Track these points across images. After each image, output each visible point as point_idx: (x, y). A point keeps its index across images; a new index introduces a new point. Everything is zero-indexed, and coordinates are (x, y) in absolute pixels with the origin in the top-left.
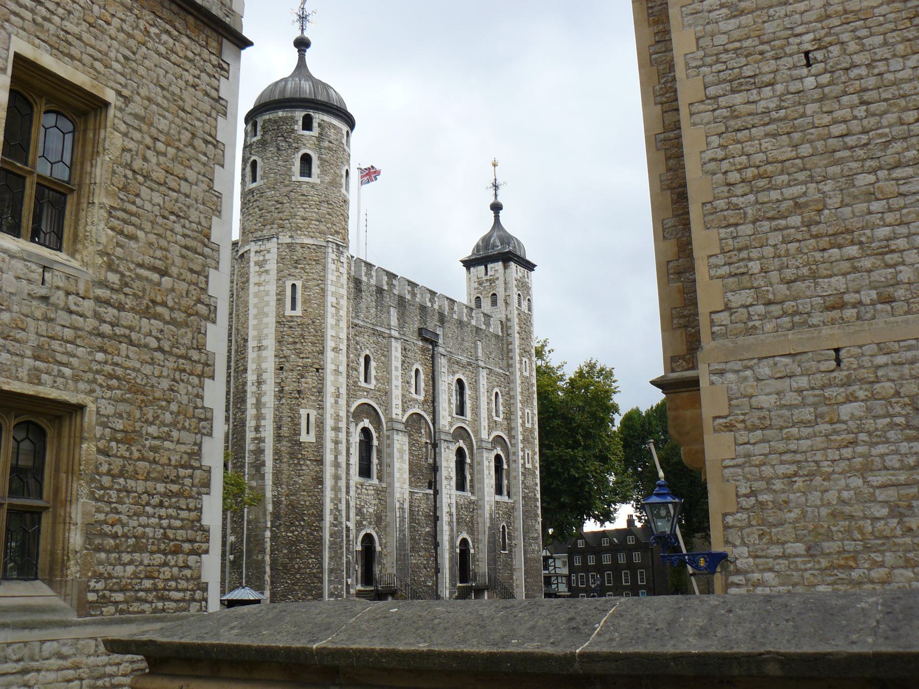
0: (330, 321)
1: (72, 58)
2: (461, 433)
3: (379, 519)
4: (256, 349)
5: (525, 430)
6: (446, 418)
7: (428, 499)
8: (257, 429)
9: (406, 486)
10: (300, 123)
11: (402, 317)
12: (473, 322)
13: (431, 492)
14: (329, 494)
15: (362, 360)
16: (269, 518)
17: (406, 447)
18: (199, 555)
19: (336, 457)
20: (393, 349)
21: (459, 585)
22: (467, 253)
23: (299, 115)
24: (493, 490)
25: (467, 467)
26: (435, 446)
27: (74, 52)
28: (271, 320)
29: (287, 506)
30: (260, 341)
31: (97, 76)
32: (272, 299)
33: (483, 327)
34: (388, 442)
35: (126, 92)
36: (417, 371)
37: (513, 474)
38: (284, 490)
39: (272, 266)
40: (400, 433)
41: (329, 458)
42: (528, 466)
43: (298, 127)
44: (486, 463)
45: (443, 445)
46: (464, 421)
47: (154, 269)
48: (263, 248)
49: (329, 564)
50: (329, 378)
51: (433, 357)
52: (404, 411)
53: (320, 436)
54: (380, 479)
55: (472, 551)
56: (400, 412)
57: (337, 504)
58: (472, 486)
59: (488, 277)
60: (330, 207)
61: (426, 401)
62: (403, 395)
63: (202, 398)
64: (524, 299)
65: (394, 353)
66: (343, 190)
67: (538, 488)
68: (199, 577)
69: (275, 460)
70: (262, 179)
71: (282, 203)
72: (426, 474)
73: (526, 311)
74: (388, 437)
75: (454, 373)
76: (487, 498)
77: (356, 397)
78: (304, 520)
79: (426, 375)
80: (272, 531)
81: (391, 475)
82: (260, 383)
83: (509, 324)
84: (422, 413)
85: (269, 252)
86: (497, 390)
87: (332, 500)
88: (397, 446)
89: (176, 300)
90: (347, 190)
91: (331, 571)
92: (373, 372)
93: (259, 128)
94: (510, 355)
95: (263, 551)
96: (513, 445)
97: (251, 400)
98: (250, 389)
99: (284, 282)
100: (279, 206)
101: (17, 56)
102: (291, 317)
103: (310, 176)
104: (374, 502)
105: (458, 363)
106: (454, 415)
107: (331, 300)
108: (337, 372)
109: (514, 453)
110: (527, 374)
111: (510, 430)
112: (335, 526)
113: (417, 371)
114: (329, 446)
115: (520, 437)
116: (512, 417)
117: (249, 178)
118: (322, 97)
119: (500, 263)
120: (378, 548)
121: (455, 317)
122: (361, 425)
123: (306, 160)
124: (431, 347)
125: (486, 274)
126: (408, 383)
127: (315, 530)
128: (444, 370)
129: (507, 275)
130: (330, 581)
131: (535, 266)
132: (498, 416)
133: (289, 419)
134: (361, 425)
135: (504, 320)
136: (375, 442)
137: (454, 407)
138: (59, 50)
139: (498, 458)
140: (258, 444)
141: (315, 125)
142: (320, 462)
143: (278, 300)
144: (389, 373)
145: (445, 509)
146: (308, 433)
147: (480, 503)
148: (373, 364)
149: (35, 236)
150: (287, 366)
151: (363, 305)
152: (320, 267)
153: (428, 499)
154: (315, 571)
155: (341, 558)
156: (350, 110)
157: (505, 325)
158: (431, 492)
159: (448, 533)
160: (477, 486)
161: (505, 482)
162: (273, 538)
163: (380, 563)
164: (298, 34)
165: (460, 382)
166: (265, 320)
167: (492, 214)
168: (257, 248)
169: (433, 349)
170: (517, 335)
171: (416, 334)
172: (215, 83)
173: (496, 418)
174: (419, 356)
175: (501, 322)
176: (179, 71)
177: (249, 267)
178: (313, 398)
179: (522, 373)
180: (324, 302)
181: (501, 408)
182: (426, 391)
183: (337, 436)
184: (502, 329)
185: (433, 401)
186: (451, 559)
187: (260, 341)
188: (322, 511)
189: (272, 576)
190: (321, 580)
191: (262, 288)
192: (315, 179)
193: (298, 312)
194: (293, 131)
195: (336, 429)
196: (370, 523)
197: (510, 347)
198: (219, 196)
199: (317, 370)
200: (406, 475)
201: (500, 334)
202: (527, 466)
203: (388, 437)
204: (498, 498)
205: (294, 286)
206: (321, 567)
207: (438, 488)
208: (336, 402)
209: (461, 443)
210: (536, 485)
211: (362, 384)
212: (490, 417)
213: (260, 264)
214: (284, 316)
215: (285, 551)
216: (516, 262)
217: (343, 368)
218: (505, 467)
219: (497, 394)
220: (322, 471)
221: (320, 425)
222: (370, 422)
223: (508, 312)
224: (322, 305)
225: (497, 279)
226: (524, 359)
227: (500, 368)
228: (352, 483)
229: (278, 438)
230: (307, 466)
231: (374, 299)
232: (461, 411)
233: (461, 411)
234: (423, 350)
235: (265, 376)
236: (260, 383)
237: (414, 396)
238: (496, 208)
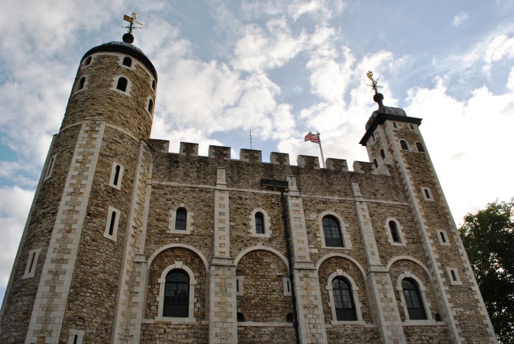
83: (398, 165)
124: (279, 193)
131: (421, 120)
144: (212, 218)
146: (30, 271)
158: (291, 324)
182: (274, 230)
201: (389, 174)
202: (453, 283)
216: (391, 119)
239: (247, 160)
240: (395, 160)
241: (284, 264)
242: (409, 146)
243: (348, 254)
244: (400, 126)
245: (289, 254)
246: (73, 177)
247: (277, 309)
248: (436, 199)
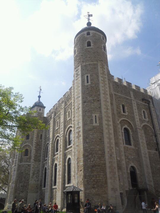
9: (146, 149)
13: (158, 152)
14: (106, 145)
19: (109, 131)
26: (156, 136)
41: (105, 131)
50: (103, 103)
53: (101, 123)
54: (135, 146)
56: (139, 123)
57: (111, 150)
65: (133, 105)
77: (120, 117)
88: (139, 134)
99: (84, 76)
108: (106, 101)
113: (144, 112)
114: (105, 127)
122: (124, 127)
124: (147, 105)
126: (141, 115)
136: (131, 133)
144: (133, 111)
146: (96, 122)
148: (126, 108)
164: (88, 22)
182: (149, 118)
193: (89, 83)
195: (108, 121)
205: (87, 76)
214: (85, 86)
215: (90, 170)
221: (101, 119)
222: (128, 126)
237: (144, 119)
239: (137, 90)
241: (152, 131)
246: (102, 87)
247: (153, 146)
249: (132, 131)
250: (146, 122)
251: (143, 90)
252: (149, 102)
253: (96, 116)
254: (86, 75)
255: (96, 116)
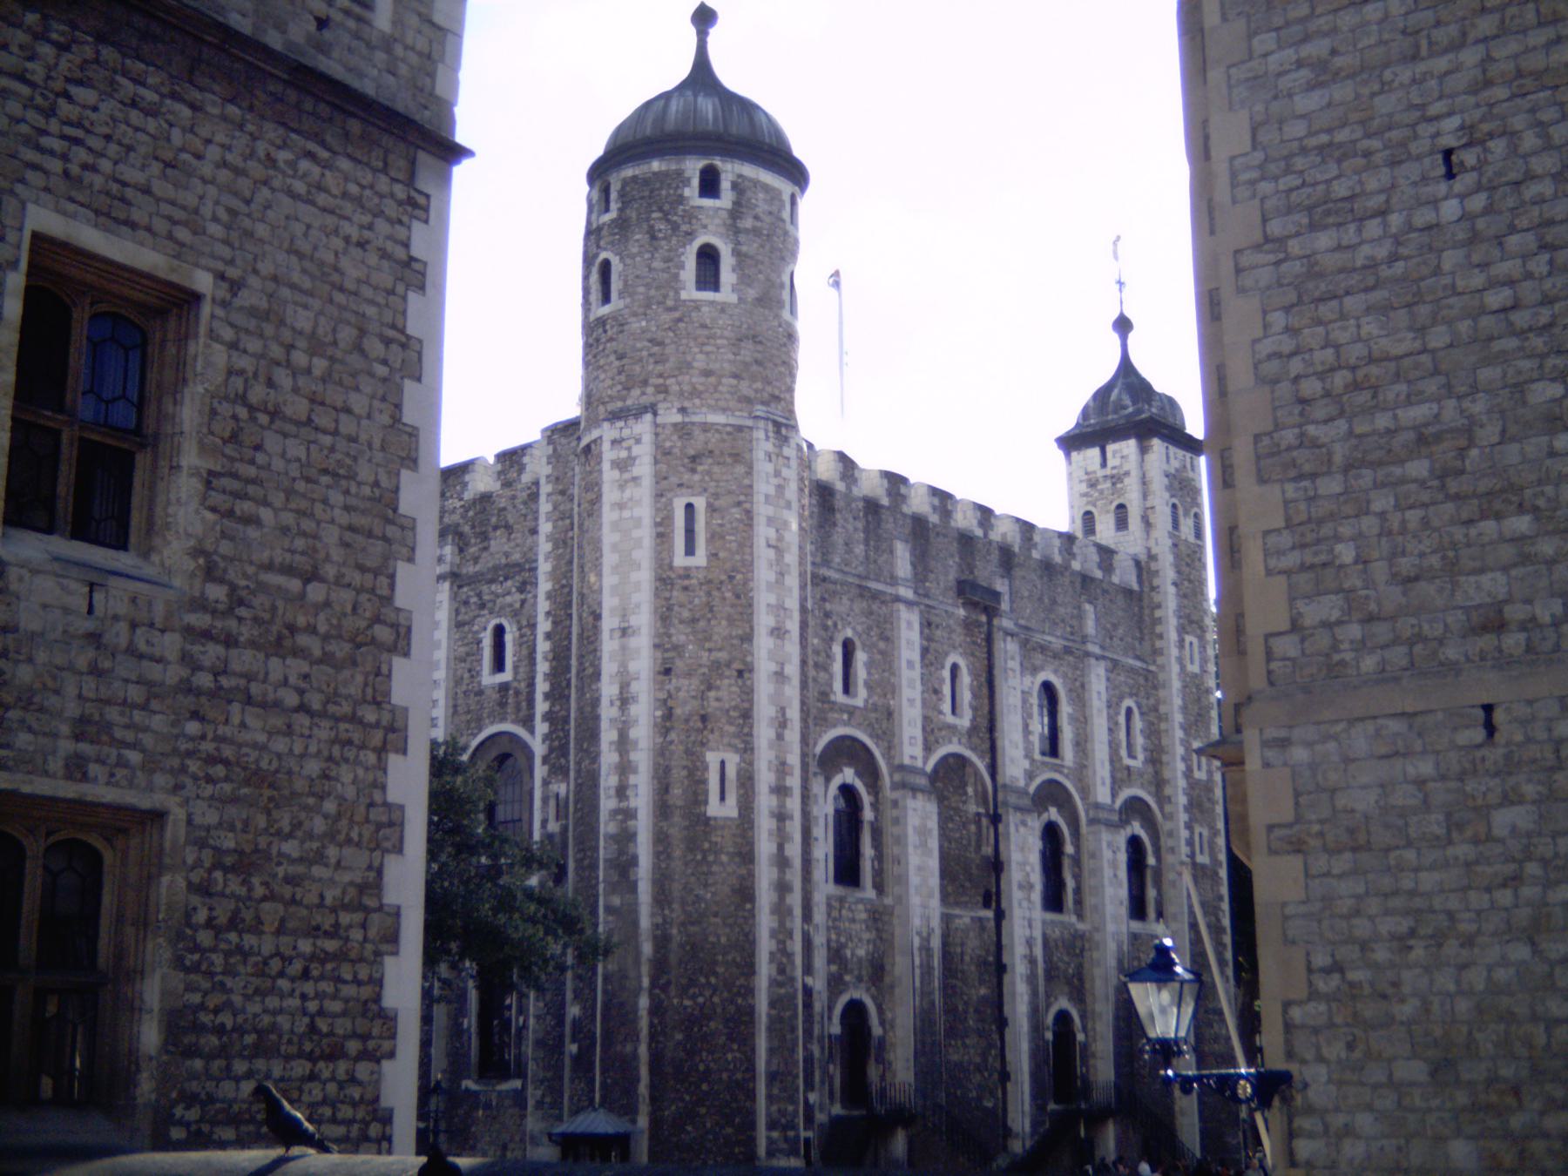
0: (764, 574)
1: (133, 225)
2: (1051, 794)
3: (877, 971)
4: (617, 634)
5: (1193, 784)
6: (1018, 760)
7: (983, 928)
8: (621, 791)
9: (935, 903)
10: (696, 182)
11: (921, 558)
12: (1076, 565)
13: (989, 914)
15: (837, 650)
16: (645, 969)
17: (933, 824)
18: (378, 1062)
19: (781, 847)
20: (903, 625)
21: (1052, 1106)
22: (1067, 421)
23: (693, 167)
24: (1124, 911)
25: (1066, 862)
26: (996, 819)
27: (137, 215)
28: (644, 576)
29: (682, 946)
30: (624, 617)
31: (180, 251)
32: (646, 534)
33: (1099, 574)
34: (895, 813)
35: (233, 273)
36: (955, 669)
37: (1170, 876)
38: (676, 913)
39: (644, 468)
40: (920, 796)
41: (765, 847)
42: (1203, 859)
43: (692, 191)
44: (1107, 854)
45: (1012, 819)
46: (1058, 769)
47: (288, 570)
48: (626, 432)
49: (768, 1062)
50: (763, 687)
51: (989, 640)
52: (928, 749)
54: (879, 887)
55: (1080, 1037)
56: (918, 751)
57: (784, 942)
58: (1079, 902)
59: (1108, 471)
60: (760, 348)
61: (973, 730)
62: (926, 719)
63: (383, 788)
64: (1186, 514)
66: (786, 314)
67: (1225, 906)
68: (377, 1099)
69: (657, 855)
70: (621, 295)
71: (661, 344)
72: (975, 876)
73: (1192, 539)
74: (895, 804)
75: (1035, 670)
76: (1111, 927)
77: (823, 722)
78: (715, 974)
79: (974, 674)
80: (652, 996)
81: (902, 880)
82: (625, 701)
83: (1153, 566)
84: (968, 753)
85: (638, 441)
86: (1129, 702)
87: (773, 934)
88: (913, 821)
89: (335, 622)
90: (793, 312)
91: (772, 1077)
92: (860, 673)
93: (613, 195)
94: (1158, 629)
95: (636, 1039)
96: (1169, 817)
97: (608, 735)
98: (608, 712)
99: (670, 502)
100: (656, 349)
101: (36, 236)
102: (687, 569)
103: (716, 288)
104: (866, 936)
105: (1043, 649)
106: (1037, 756)
107: (763, 532)
109: (1170, 834)
110: (1194, 668)
111: (1159, 784)
112: (780, 985)
113: (955, 669)
114: (764, 825)
115: (1182, 800)
116: (1165, 758)
117: (595, 296)
118: (738, 127)
119: (1132, 443)
120: (877, 1030)
121: (1036, 555)
122: (837, 781)
123: (708, 256)
124: (984, 618)
125: (1104, 464)
126: (936, 692)
127: (738, 994)
128: (1014, 664)
129: (1147, 466)
130: (770, 1097)
132: (1132, 756)
133: (685, 773)
134: (837, 781)
135: (1143, 558)
136: (868, 814)
137: (1035, 740)
138: (111, 215)
139: (1135, 844)
140: (624, 821)
141: (725, 185)
142: (747, 856)
143: (660, 535)
145: (1020, 950)
146: (722, 798)
147: (1097, 937)
148: (860, 657)
149: (80, 532)
150: (679, 665)
151: (838, 537)
152: (740, 469)
153: (983, 928)
154: (739, 1076)
155: (793, 1050)
156: (798, 152)
157: (1144, 568)
158: (989, 914)
159: (1026, 998)
160: (1089, 901)
161: (1151, 893)
162: (656, 1009)
163: (880, 1060)
165: (1048, 688)
166: (634, 576)
167: (1115, 338)
168: (615, 434)
169: (990, 623)
170: (1172, 590)
171: (952, 594)
172: (401, 232)
173: (1131, 762)
174: (959, 637)
175: (1138, 563)
176: (330, 221)
177: (600, 471)
178: (732, 729)
179: (1183, 667)
180: (751, 538)
181: (1139, 741)
182: (975, 709)
183: (782, 805)
184: (1139, 576)
185: (992, 728)
186: (1034, 1055)
187: (624, 617)
188: (752, 955)
189: (652, 1086)
190: (751, 1095)
191: (626, 514)
192: (726, 295)
193: (700, 559)
194: (681, 199)
196: (859, 979)
197: (1158, 613)
198: (413, 433)
199: (740, 673)
200: (935, 881)
201: (1136, 587)
203: (895, 804)
204: (1136, 926)
205: (689, 507)
206: (751, 1069)
207: (1004, 905)
208: (780, 737)
209: (1053, 814)
210: (1221, 898)
211: (838, 696)
212: (1114, 758)
213: (622, 465)
214: (671, 567)
216: (1164, 438)
217: (793, 670)
218: (1151, 861)
219: (1129, 711)
220: (751, 874)
221: (747, 781)
222: (858, 774)
223: (1152, 543)
224: (746, 543)
225: (1127, 474)
226: (1188, 639)
227: (1137, 658)
228: (819, 898)
229: (662, 809)
230: (722, 864)
231: (860, 525)
232: (1052, 746)
233: (1052, 746)
234: (968, 625)
235: (635, 687)
236: (625, 701)
237: (950, 719)
238: (1123, 325)
240: (1149, 550)
242: (1182, 519)
243: (1067, 776)
244: (1177, 454)
245: (993, 769)
248: (1201, 667)
249: (875, 806)
250: (955, 740)
251: (970, 513)
252: (996, 595)
253: (723, 763)
254: (685, 500)
255: (723, 763)
